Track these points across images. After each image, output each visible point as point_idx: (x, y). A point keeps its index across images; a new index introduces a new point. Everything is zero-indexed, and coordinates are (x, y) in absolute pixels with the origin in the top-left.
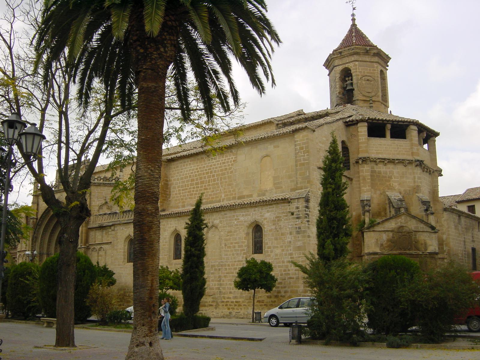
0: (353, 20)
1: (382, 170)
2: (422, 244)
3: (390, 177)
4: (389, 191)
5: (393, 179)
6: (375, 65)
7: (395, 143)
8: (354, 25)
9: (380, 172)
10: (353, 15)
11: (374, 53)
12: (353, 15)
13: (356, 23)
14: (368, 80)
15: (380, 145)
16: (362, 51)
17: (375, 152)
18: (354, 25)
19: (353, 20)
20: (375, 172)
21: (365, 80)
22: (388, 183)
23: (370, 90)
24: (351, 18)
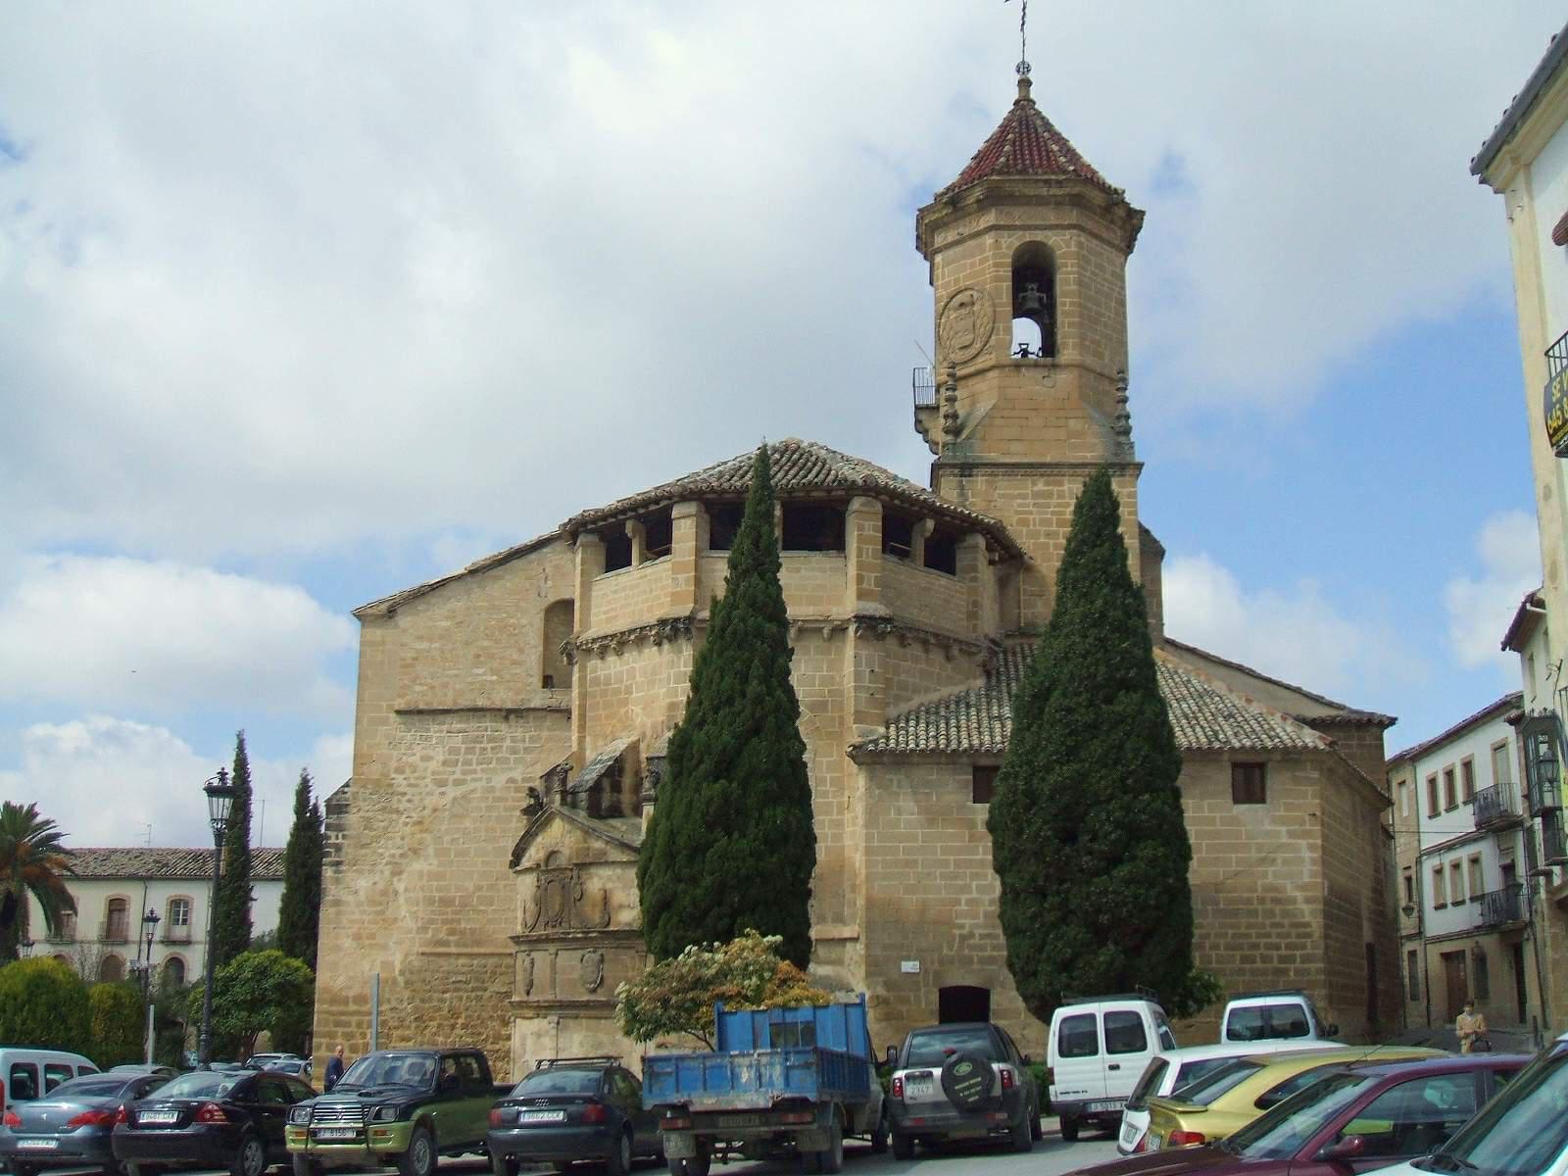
0: (1024, 84)
1: (613, 671)
2: (594, 906)
3: (629, 691)
4: (623, 734)
5: (635, 695)
6: (988, 240)
7: (646, 576)
8: (1024, 103)
9: (608, 678)
10: (1023, 68)
11: (978, 201)
12: (1023, 68)
13: (1032, 96)
14: (962, 305)
15: (615, 592)
16: (944, 212)
17: (604, 616)
18: (1024, 103)
19: (1024, 84)
20: (596, 681)
21: (956, 309)
22: (623, 711)
23: (967, 339)
24: (1018, 77)
